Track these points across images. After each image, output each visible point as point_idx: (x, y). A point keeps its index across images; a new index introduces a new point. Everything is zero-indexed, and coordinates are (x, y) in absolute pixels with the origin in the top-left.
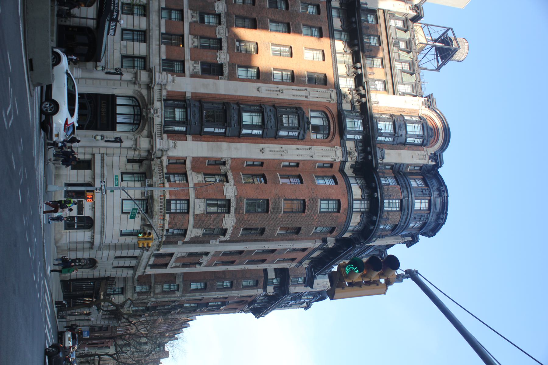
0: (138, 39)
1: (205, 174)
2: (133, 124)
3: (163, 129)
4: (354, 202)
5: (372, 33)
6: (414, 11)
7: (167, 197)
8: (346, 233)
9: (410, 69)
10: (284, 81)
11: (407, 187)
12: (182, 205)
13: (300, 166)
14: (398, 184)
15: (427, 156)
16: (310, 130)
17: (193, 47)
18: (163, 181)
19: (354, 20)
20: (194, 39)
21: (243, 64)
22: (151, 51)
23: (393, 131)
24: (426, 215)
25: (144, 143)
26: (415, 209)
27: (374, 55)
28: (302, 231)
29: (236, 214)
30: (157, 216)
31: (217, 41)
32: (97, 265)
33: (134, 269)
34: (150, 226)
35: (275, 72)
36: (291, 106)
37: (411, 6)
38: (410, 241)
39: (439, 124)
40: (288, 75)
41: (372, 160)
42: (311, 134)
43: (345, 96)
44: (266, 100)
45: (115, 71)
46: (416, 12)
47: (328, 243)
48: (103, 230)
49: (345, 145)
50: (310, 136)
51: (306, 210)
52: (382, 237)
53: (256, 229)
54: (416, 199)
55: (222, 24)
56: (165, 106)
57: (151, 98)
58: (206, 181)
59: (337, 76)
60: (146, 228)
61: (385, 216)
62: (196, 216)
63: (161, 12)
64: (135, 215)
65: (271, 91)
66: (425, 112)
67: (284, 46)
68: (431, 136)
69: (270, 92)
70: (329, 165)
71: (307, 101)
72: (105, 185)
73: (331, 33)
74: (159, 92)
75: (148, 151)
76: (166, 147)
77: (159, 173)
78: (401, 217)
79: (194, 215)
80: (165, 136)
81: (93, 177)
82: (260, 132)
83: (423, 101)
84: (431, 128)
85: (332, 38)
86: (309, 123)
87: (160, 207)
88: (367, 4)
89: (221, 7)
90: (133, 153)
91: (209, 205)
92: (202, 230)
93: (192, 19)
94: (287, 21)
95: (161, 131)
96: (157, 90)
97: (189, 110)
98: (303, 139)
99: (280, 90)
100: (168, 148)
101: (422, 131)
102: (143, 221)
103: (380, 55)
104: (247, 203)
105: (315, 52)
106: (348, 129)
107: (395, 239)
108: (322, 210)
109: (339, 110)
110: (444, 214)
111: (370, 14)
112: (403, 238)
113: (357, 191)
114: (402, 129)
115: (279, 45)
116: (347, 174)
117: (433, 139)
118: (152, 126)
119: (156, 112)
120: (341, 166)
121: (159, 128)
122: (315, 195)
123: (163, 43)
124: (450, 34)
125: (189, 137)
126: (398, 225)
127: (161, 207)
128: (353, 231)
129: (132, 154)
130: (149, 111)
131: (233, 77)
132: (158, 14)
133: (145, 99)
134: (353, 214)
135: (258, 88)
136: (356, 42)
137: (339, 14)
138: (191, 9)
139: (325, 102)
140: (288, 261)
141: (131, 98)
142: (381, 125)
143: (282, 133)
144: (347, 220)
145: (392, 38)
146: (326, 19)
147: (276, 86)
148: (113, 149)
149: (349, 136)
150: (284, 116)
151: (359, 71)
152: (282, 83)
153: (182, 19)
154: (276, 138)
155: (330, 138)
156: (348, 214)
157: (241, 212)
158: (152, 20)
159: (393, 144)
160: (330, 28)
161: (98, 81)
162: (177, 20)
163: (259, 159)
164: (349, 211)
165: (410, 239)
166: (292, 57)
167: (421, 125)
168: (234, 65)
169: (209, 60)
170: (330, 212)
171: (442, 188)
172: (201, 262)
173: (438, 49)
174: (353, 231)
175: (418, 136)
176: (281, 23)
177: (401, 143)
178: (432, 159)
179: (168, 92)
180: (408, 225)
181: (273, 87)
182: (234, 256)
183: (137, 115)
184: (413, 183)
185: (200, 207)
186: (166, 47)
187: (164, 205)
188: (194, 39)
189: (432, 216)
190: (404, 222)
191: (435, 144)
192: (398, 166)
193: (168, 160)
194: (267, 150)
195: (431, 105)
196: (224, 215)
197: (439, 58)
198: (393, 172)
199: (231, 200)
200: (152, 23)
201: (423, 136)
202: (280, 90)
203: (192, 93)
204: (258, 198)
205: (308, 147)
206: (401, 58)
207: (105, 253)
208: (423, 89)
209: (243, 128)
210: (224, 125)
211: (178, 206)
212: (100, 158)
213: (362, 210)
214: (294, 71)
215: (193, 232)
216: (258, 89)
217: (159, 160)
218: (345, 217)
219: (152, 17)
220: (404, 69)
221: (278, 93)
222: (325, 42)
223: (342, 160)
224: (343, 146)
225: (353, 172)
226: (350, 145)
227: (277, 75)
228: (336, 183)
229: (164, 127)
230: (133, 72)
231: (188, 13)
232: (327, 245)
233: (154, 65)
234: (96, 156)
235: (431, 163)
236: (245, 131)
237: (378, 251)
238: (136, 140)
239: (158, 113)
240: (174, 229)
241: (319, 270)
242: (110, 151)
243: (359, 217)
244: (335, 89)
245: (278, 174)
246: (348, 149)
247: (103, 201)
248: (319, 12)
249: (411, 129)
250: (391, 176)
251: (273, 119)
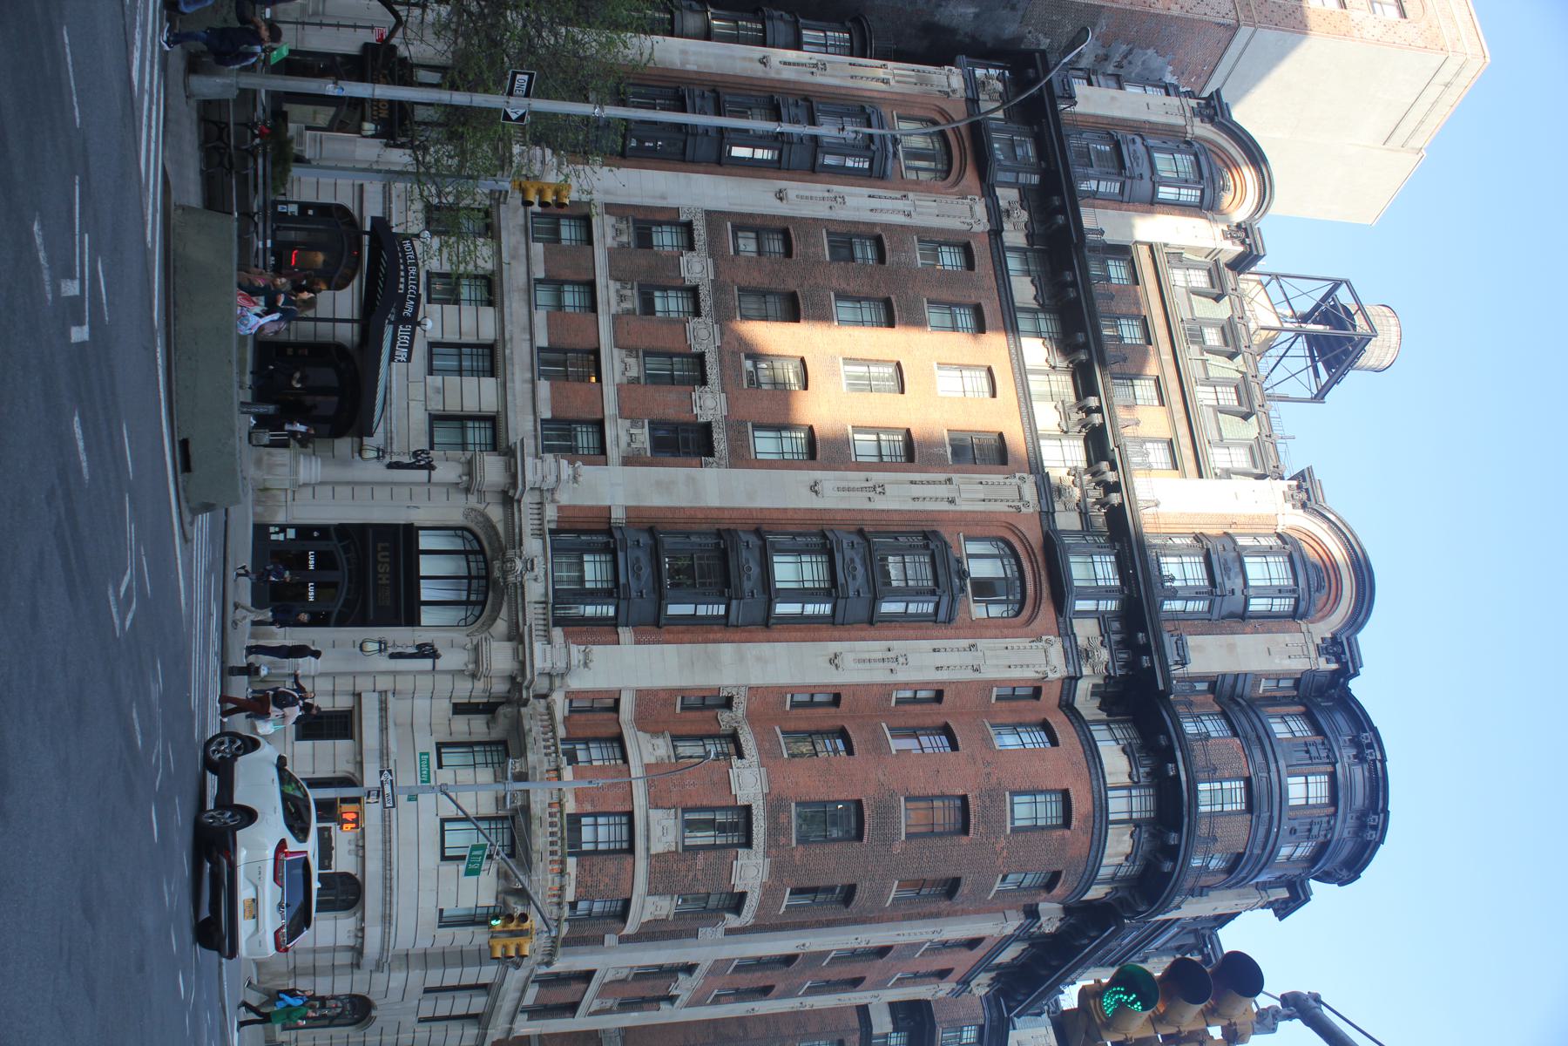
0: (475, 368)
1: (676, 738)
2: (467, 603)
3: (550, 613)
4: (1110, 794)
5: (1124, 309)
6: (1237, 242)
7: (570, 807)
8: (1093, 887)
9: (1240, 404)
10: (885, 459)
11: (1261, 740)
12: (612, 828)
13: (945, 698)
14: (1235, 734)
15: (1312, 648)
16: (967, 596)
17: (625, 380)
18: (556, 761)
19: (1068, 277)
20: (626, 360)
21: (766, 420)
22: (509, 398)
23: (1206, 583)
24: (1325, 819)
25: (500, 658)
26: (1292, 803)
27: (1133, 371)
28: (964, 889)
29: (770, 847)
30: (541, 864)
31: (690, 360)
32: (374, 1013)
33: (479, 1023)
34: (523, 895)
35: (857, 437)
36: (908, 529)
37: (1226, 229)
38: (1285, 901)
39: (1339, 553)
40: (897, 443)
41: (1152, 669)
42: (973, 606)
43: (1060, 491)
44: (838, 517)
45: (413, 460)
46: (1243, 243)
47: (1043, 919)
48: (388, 912)
49: (1072, 630)
50: (969, 612)
51: (972, 826)
52: (1200, 891)
53: (830, 890)
54: (1291, 775)
55: (703, 313)
56: (553, 549)
57: (514, 530)
58: (677, 758)
59: (1034, 436)
60: (511, 900)
61: (1203, 829)
62: (655, 859)
63: (535, 290)
64: (481, 863)
65: (849, 489)
66: (1295, 520)
67: (877, 362)
68: (1319, 588)
69: (846, 494)
70: (1029, 691)
71: (955, 512)
72: (391, 781)
73: (1007, 317)
74: (536, 511)
75: (512, 679)
76: (561, 665)
77: (544, 740)
78: (1252, 831)
79: (649, 855)
80: (557, 633)
81: (358, 759)
82: (825, 609)
83: (1286, 489)
84: (1315, 566)
85: (1013, 331)
86: (963, 574)
87: (550, 839)
88: (1102, 232)
89: (697, 268)
90: (468, 685)
91: (690, 825)
92: (672, 899)
93: (618, 305)
94: (882, 293)
95: (544, 620)
96: (531, 506)
97: (621, 555)
98: (950, 620)
99: (874, 488)
100: (568, 667)
101: (1290, 575)
102: (502, 881)
103: (1152, 369)
104: (799, 815)
105: (965, 373)
106: (1076, 583)
107: (1240, 896)
108: (1017, 823)
109: (1047, 532)
110: (1378, 815)
111: (1115, 259)
112: (1263, 893)
113: (1115, 763)
114: (1232, 575)
115: (865, 360)
116: (1083, 713)
117: (1325, 598)
118: (520, 606)
119: (529, 566)
120: (1065, 692)
121: (541, 611)
122: (994, 780)
123: (542, 374)
124: (1343, 296)
125: (625, 633)
126: (1244, 853)
127: (555, 839)
128: (1113, 879)
129: (465, 690)
130: (509, 565)
131: (741, 457)
132: (526, 297)
133: (497, 533)
134: (1110, 831)
135: (813, 484)
136: (1081, 337)
137: (1028, 265)
138: (617, 279)
139: (1005, 513)
140: (927, 979)
141: (459, 533)
142: (1170, 566)
143: (888, 607)
144: (1094, 848)
145: (1182, 320)
146: (991, 282)
147: (863, 475)
148: (412, 677)
149: (1081, 605)
150: (891, 559)
151: (1096, 419)
152: (880, 464)
153: (593, 307)
154: (873, 621)
155: (1026, 613)
156: (1096, 832)
157: (782, 840)
158: (511, 315)
159: (1210, 620)
160: (1005, 304)
161: (368, 489)
162: (577, 310)
163: (828, 686)
164: (1097, 821)
165: (1283, 893)
166: (903, 392)
167: (1286, 559)
168: (743, 423)
169: (672, 413)
170: (1043, 828)
171: (1366, 737)
172: (674, 992)
173: (1313, 341)
174: (1112, 879)
175: (1280, 591)
176: (867, 299)
177: (1232, 616)
178: (1328, 653)
179: (560, 508)
180: (1274, 852)
181: (856, 478)
182: (768, 973)
183: (478, 578)
184: (1279, 729)
185: (664, 831)
186: (551, 385)
187: (562, 833)
188: (626, 360)
189: (1344, 821)
190: (1261, 844)
191: (1331, 612)
192: (1229, 681)
193: (567, 701)
194: (848, 660)
195: (1309, 499)
196: (734, 853)
197: (1320, 366)
198: (1218, 700)
199: (754, 806)
200: (512, 323)
201: (1294, 591)
202: (874, 488)
203: (627, 508)
204: (831, 798)
205: (965, 643)
206: (1211, 374)
207: (397, 979)
208: (1282, 455)
209: (778, 600)
210: (722, 594)
211: (602, 831)
212: (376, 705)
213: (1135, 816)
214: (912, 431)
215: (647, 907)
216: (814, 488)
217: (542, 701)
218: (1084, 839)
219: (511, 306)
220: (1221, 402)
221: (871, 494)
222: (995, 345)
223: (1065, 674)
224: (1067, 635)
225: (1100, 708)
226: (1086, 630)
227: (864, 444)
228: (1054, 741)
229: (554, 609)
230: (463, 459)
231: (607, 290)
232: (1041, 925)
233: (520, 438)
234: (364, 701)
235: (1325, 665)
236: (782, 609)
237: (1192, 935)
238: (476, 648)
239: (536, 570)
240: (593, 901)
241: (1020, 1003)
242: (404, 684)
243: (1127, 837)
244: (1031, 473)
245: (884, 725)
246: (1081, 641)
247: (387, 829)
248: (970, 264)
249: (1259, 572)
250: (1212, 711)
251: (860, 571)
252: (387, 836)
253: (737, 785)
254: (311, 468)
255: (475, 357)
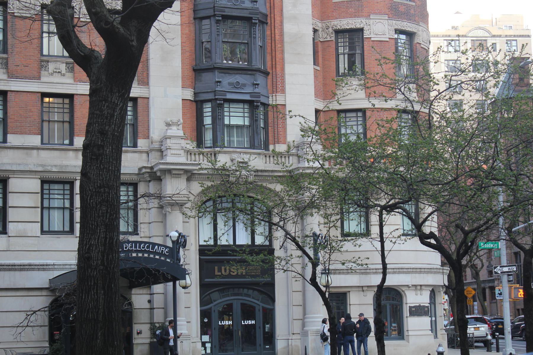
17: (70, 75)
20: (51, 71)
72: (501, 267)
96: (268, 162)
97: (229, 96)
186: (78, 136)
252: (418, 270)
253: (382, 36)
254: (182, 325)
255: (51, 196)
